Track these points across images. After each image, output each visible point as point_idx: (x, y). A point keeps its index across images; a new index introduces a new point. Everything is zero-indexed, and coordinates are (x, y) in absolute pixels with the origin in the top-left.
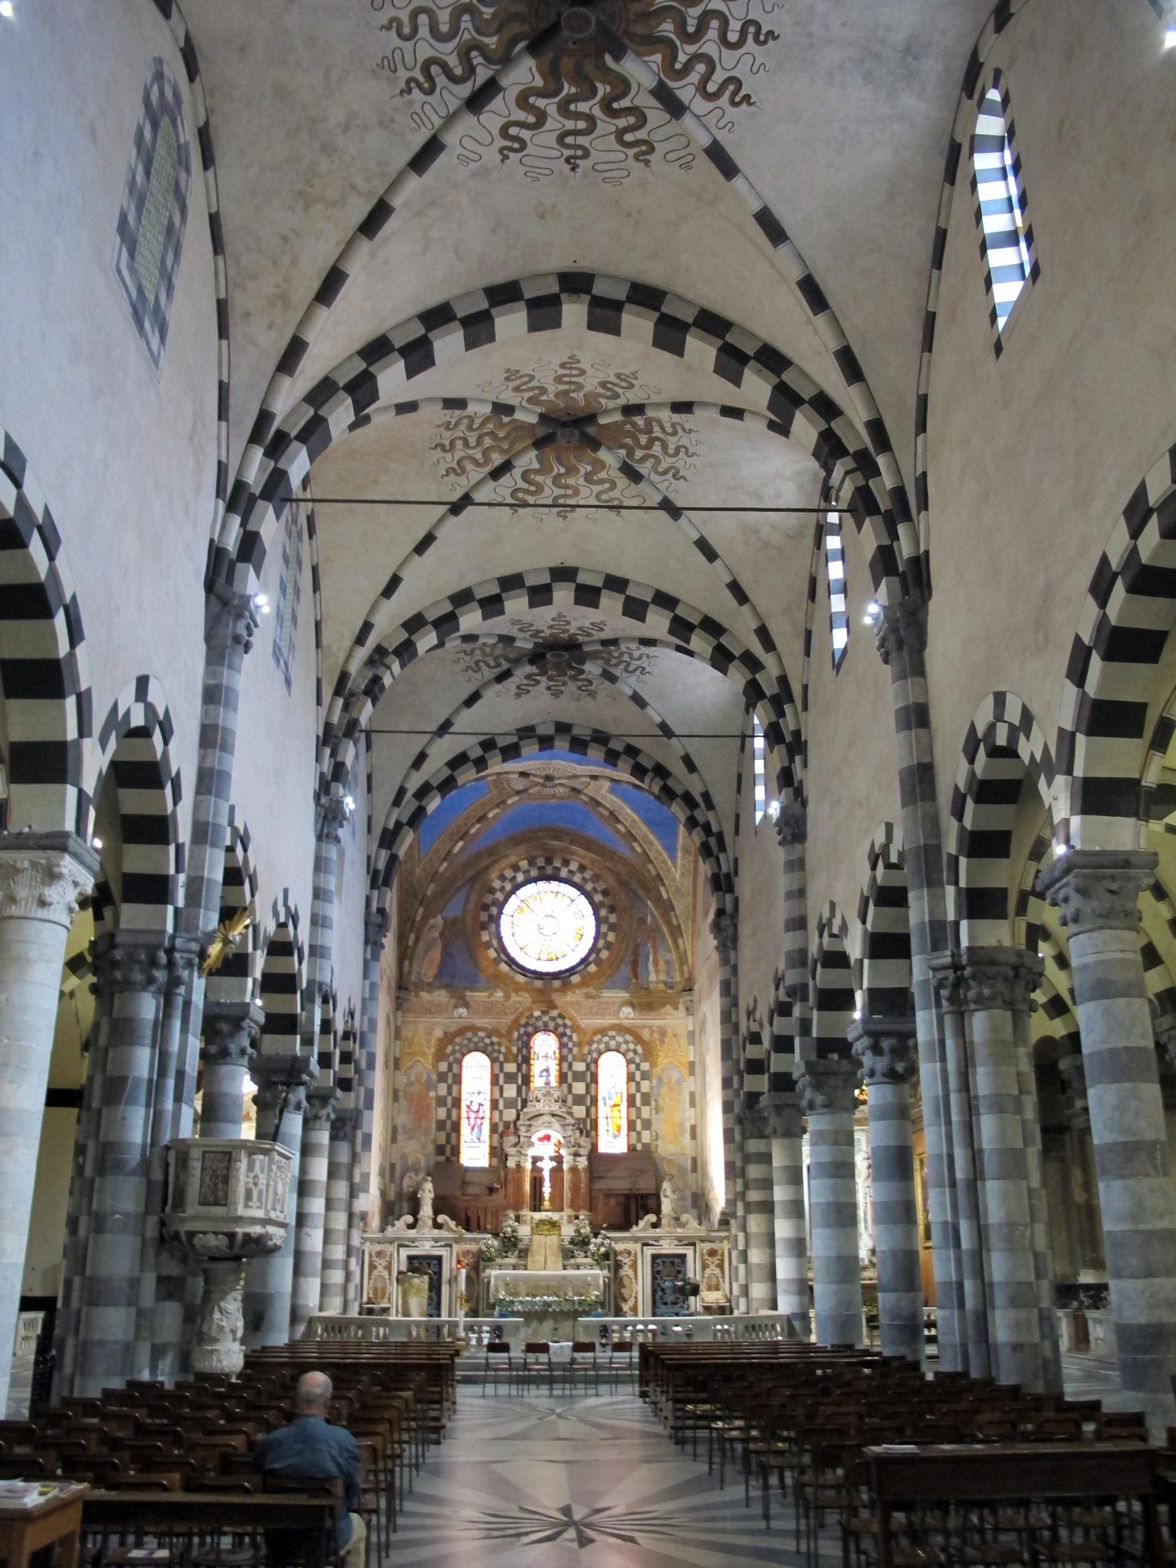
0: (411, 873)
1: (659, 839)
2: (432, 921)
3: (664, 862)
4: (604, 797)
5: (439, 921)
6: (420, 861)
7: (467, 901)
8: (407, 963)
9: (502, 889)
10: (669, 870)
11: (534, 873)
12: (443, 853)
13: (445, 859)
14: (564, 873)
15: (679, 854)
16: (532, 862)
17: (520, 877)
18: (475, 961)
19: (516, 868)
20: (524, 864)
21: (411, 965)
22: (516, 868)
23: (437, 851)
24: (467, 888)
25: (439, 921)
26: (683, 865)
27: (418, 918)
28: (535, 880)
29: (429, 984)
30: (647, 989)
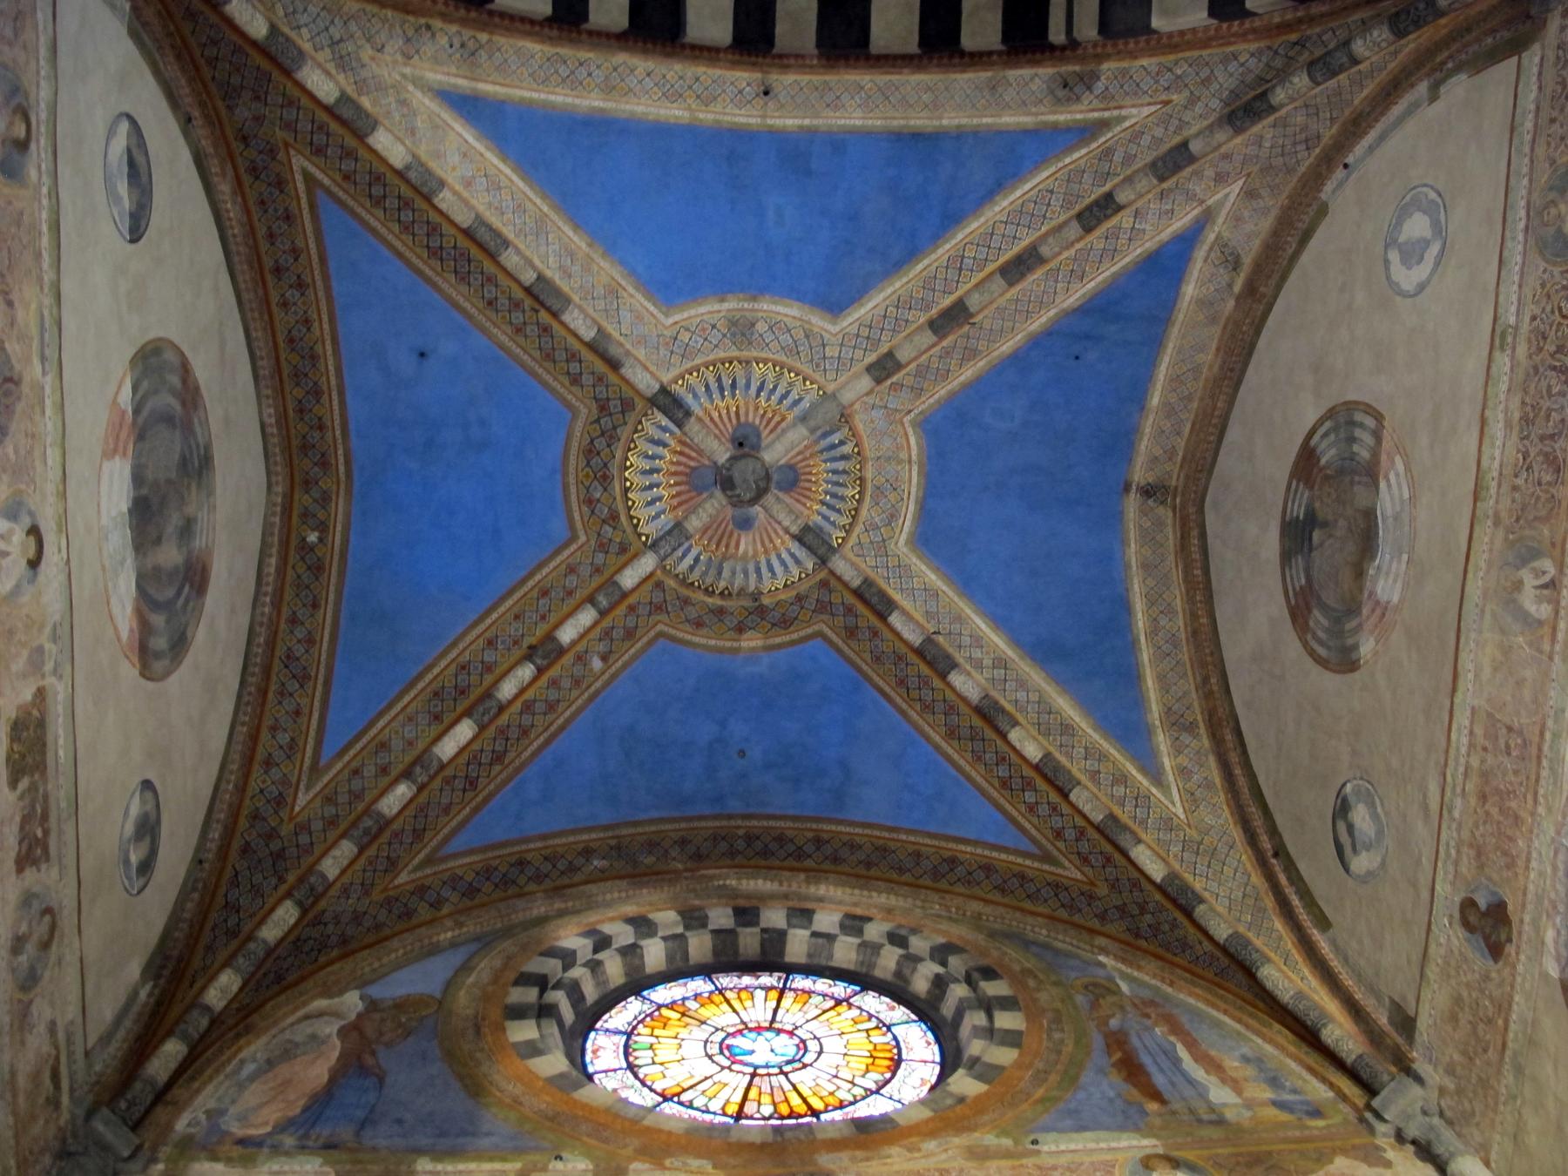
0: (280, 801)
1: (1088, 705)
2: (321, 1003)
3: (1122, 779)
4: (903, 570)
5: (352, 1002)
6: (316, 770)
7: (465, 968)
8: (172, 1050)
9: (595, 966)
10: (1141, 799)
11: (699, 946)
12: (400, 762)
13: (407, 774)
14: (798, 945)
15: (1162, 741)
16: (693, 919)
17: (654, 954)
18: (475, 1088)
19: (643, 926)
20: (668, 918)
21: (185, 1070)
22: (643, 926)
23: (383, 746)
24: (473, 947)
25: (352, 1002)
26: (1183, 772)
27: (270, 933)
28: (707, 971)
29: (242, 1142)
30: (1220, 1122)
